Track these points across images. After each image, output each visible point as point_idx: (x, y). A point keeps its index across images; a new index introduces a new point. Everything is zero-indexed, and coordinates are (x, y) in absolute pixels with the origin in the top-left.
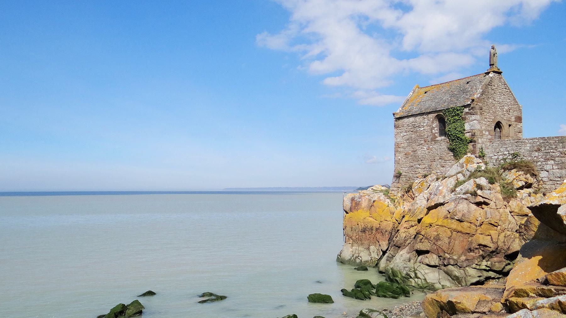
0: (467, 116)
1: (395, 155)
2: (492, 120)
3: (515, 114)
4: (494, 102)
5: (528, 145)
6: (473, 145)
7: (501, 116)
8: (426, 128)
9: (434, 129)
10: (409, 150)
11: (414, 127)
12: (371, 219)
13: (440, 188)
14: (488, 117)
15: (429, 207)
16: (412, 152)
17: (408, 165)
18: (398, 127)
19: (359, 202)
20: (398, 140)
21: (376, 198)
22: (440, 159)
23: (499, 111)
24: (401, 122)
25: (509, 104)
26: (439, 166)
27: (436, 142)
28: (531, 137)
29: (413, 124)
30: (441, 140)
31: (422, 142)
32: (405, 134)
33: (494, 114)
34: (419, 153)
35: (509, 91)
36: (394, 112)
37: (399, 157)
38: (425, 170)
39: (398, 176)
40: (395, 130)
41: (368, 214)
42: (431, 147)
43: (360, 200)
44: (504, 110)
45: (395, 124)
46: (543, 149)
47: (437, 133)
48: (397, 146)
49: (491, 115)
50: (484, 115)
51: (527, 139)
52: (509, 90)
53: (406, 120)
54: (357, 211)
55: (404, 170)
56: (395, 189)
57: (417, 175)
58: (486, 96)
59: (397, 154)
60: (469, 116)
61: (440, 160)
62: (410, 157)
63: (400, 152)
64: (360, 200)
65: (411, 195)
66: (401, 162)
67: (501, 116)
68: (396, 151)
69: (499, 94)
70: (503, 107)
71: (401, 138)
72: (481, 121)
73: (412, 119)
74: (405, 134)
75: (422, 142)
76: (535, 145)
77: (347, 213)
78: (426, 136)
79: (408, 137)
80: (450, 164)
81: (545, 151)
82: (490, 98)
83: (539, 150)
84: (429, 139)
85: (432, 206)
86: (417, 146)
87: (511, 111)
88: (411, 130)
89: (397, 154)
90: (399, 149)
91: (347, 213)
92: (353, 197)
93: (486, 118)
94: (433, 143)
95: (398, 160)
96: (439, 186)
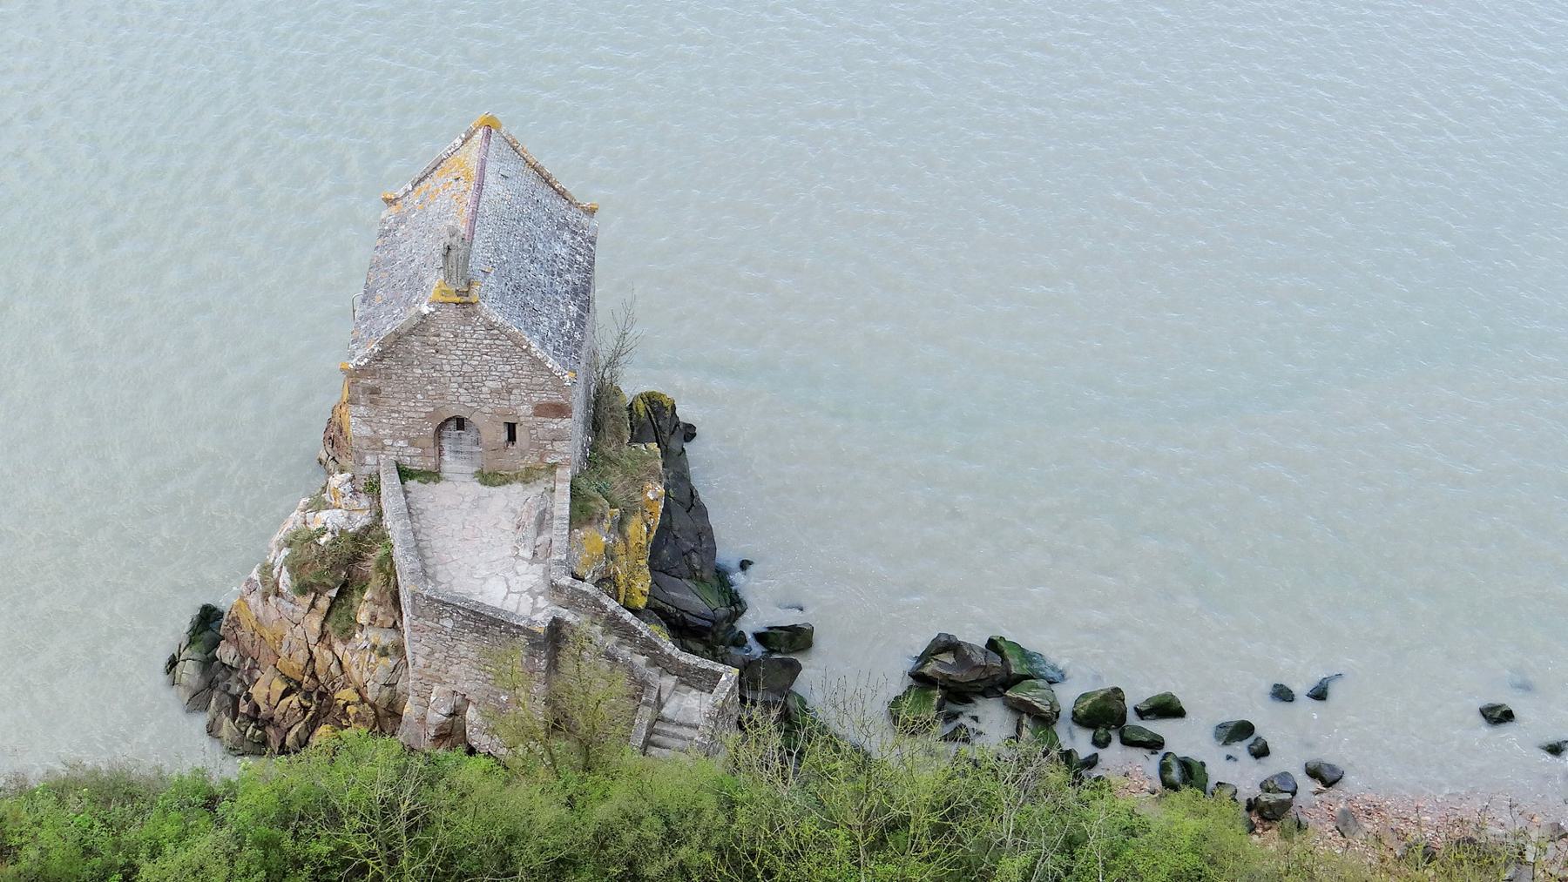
2: (423, 415)
3: (535, 400)
44: (484, 389)
87: (515, 391)
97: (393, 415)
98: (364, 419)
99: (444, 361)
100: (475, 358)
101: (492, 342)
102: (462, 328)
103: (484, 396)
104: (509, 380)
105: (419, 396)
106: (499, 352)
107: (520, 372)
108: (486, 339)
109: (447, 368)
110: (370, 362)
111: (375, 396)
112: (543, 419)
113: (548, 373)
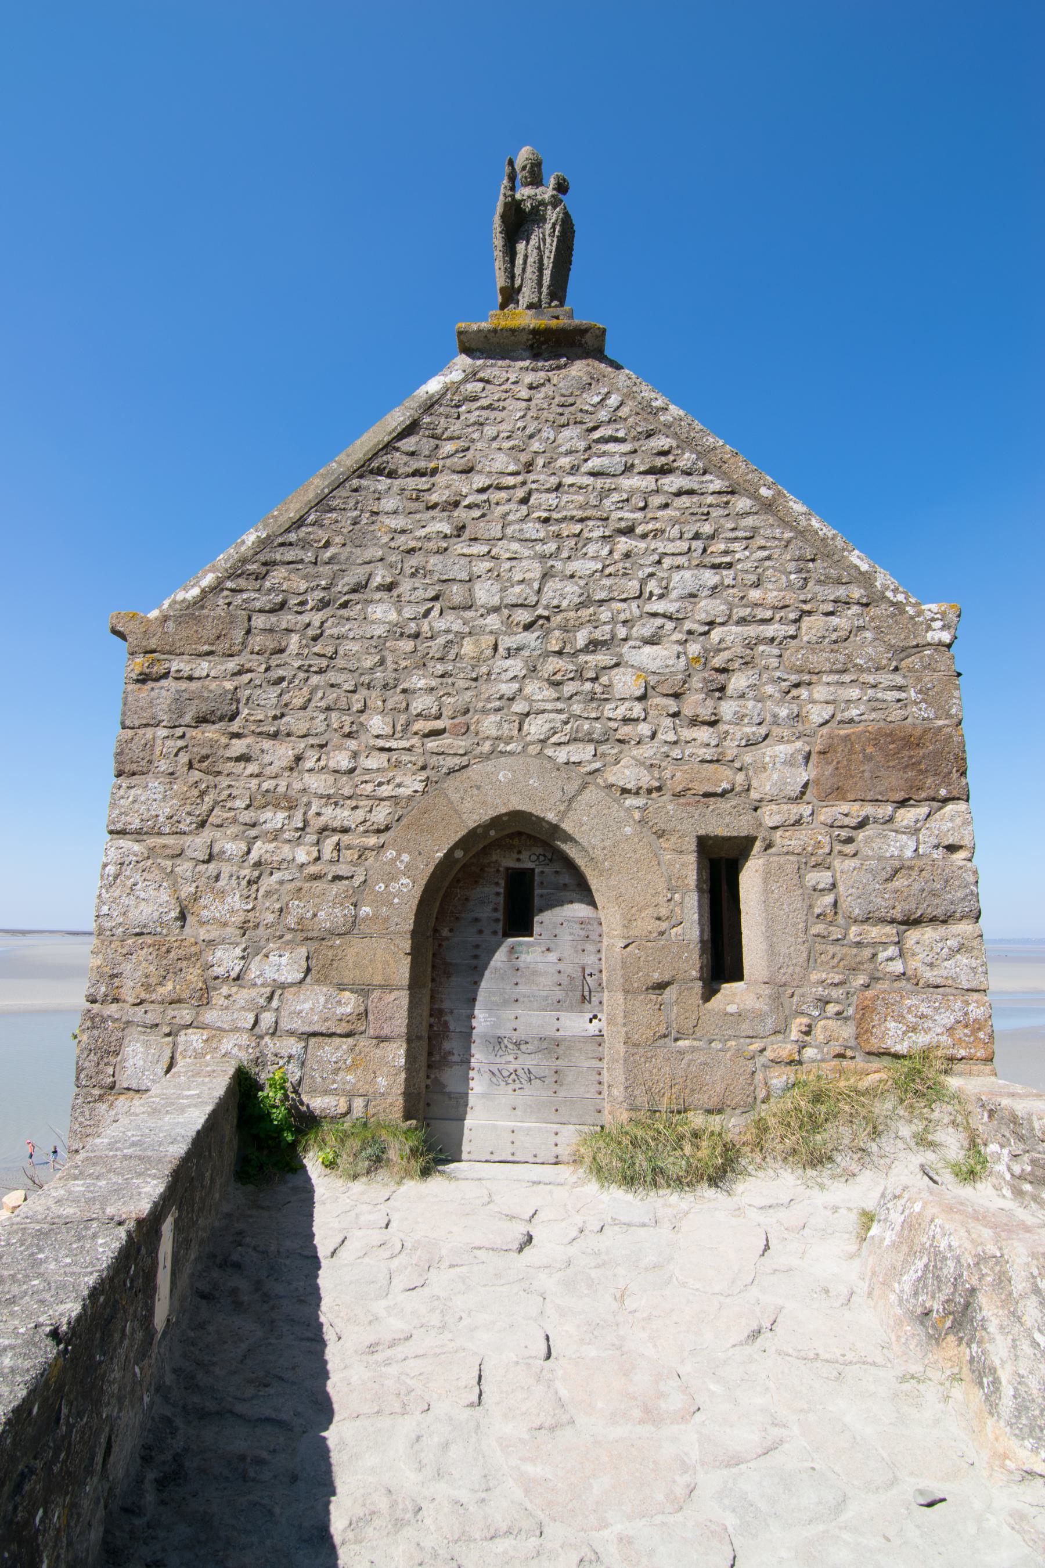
2: (381, 815)
3: (817, 714)
4: (441, 625)
7: (562, 755)
14: (317, 783)
23: (519, 707)
25: (709, 607)
33: (432, 744)
35: (718, 485)
49: (376, 761)
50: (252, 768)
52: (724, 475)
58: (305, 577)
67: (562, 755)
69: (532, 529)
70: (602, 658)
82: (390, 587)
87: (738, 682)
97: (268, 814)
98: (152, 841)
99: (481, 567)
100: (591, 549)
101: (649, 482)
102: (548, 433)
103: (621, 711)
104: (716, 634)
105: (377, 723)
106: (674, 522)
107: (755, 594)
108: (628, 469)
109: (485, 593)
110: (217, 588)
111: (210, 732)
112: (858, 811)
113: (857, 593)
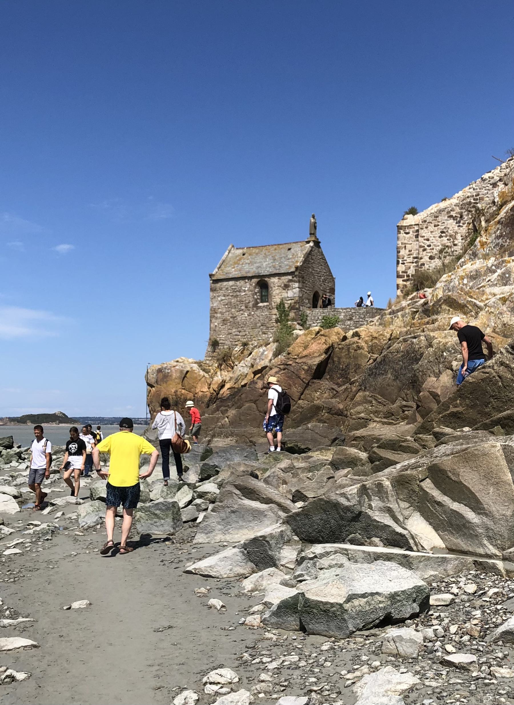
0: (290, 284)
1: (211, 321)
5: (343, 314)
6: (295, 313)
8: (247, 292)
9: (256, 295)
10: (227, 316)
11: (234, 291)
12: (183, 391)
13: (266, 353)
15: (256, 371)
16: (231, 317)
17: (226, 332)
18: (215, 290)
19: (168, 373)
20: (215, 305)
21: (188, 369)
22: (262, 325)
24: (218, 285)
26: (260, 333)
27: (258, 308)
28: (345, 307)
29: (233, 287)
30: (264, 306)
31: (243, 308)
32: (223, 298)
34: (239, 319)
36: (211, 273)
37: (216, 324)
38: (245, 337)
39: (215, 344)
40: (211, 294)
41: (180, 386)
42: (253, 313)
43: (169, 371)
45: (211, 286)
46: (354, 318)
47: (258, 299)
48: (214, 311)
51: (342, 309)
53: (225, 283)
54: (166, 383)
55: (221, 337)
56: (210, 358)
57: (236, 343)
59: (213, 320)
60: (293, 283)
61: (262, 327)
62: (229, 324)
63: (217, 318)
64: (169, 371)
65: (230, 364)
66: (217, 329)
68: (212, 317)
71: (218, 302)
72: (303, 290)
73: (231, 283)
74: (223, 298)
75: (243, 308)
76: (347, 314)
77: (152, 388)
78: (247, 302)
79: (226, 301)
80: (272, 331)
81: (355, 320)
83: (350, 319)
84: (251, 304)
85: (260, 369)
86: (237, 311)
88: (231, 294)
89: (213, 320)
90: (216, 315)
91: (152, 386)
92: (160, 369)
93: (306, 287)
94: (255, 309)
95: (214, 326)
96: (264, 351)
